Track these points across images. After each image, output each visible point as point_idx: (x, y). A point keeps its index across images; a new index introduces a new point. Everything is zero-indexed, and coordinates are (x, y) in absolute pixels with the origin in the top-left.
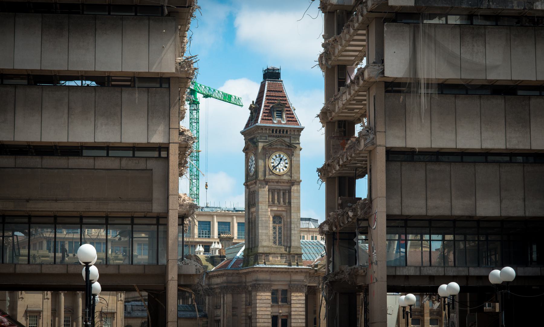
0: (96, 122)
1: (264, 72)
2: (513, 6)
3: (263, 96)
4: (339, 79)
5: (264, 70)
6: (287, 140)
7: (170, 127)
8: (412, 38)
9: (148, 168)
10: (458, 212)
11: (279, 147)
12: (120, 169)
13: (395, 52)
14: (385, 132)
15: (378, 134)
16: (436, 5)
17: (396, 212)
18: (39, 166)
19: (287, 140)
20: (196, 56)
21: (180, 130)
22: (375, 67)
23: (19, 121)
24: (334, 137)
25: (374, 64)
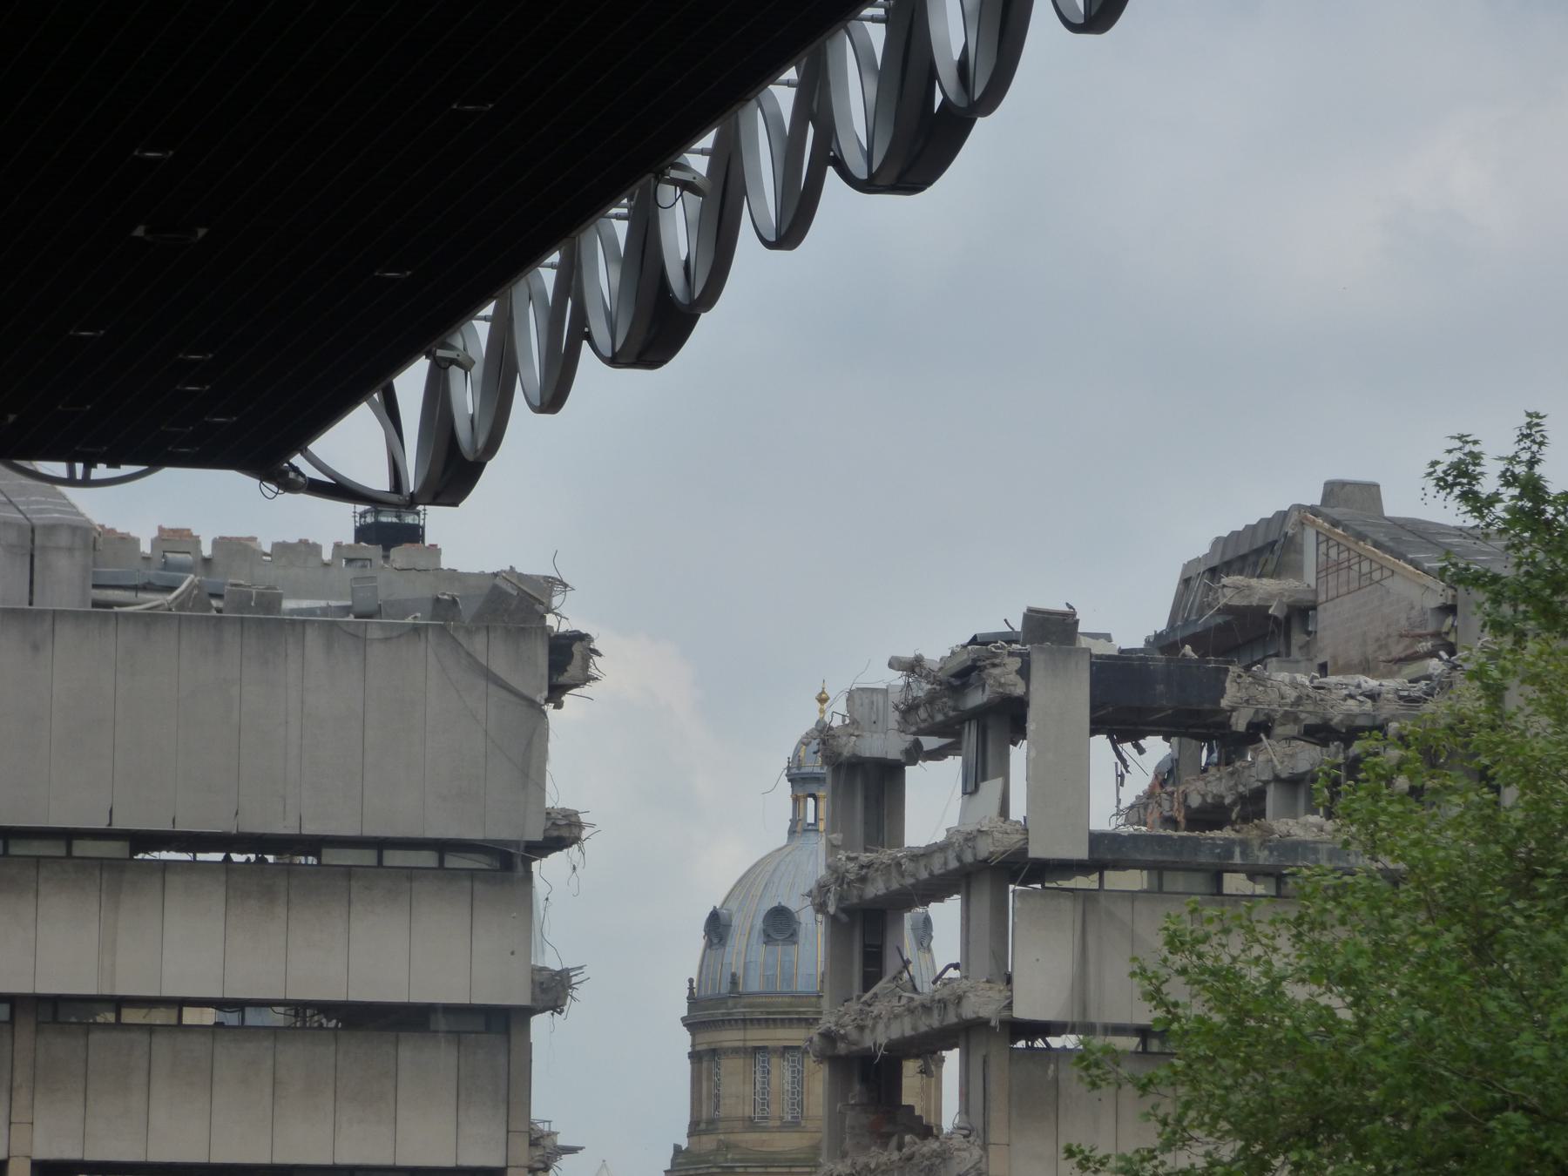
0: (337, 1114)
1: (357, 519)
4: (865, 946)
7: (510, 1129)
8: (1078, 926)
13: (1038, 960)
14: (1008, 1145)
15: (992, 1148)
16: (1138, 857)
20: (581, 968)
21: (530, 1135)
22: (990, 993)
24: (852, 1105)
25: (988, 985)
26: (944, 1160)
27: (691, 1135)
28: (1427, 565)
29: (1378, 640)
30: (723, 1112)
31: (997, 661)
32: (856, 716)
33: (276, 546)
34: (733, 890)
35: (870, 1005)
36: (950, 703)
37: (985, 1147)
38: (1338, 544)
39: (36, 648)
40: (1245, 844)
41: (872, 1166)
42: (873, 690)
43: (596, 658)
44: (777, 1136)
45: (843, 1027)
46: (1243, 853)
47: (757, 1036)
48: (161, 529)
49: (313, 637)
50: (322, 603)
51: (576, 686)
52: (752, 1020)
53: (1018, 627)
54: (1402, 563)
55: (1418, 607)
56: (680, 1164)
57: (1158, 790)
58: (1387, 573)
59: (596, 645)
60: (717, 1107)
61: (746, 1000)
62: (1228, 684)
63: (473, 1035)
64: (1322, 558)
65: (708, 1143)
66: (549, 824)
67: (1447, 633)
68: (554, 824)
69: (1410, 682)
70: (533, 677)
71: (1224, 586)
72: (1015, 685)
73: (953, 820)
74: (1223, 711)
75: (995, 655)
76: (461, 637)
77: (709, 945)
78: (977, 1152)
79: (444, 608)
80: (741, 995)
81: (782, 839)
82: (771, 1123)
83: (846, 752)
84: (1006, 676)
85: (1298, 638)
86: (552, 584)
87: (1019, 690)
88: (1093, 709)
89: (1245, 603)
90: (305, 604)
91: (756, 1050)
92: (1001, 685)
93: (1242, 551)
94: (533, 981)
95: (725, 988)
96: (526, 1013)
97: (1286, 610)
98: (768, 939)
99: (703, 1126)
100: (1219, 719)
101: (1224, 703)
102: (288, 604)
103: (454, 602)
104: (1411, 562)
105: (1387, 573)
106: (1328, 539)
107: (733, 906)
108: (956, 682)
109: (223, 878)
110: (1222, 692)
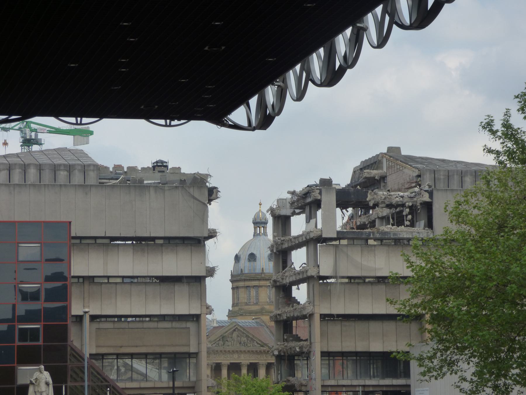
2: (390, 236)
4: (283, 259)
5: (153, 162)
9: (187, 327)
10: (359, 349)
12: (172, 328)
16: (348, 236)
17: (325, 350)
18: (127, 327)
22: (314, 270)
26: (304, 309)
27: (232, 307)
28: (413, 166)
29: (402, 184)
30: (240, 301)
31: (314, 191)
32: (279, 205)
33: (142, 168)
34: (240, 250)
35: (284, 273)
36: (303, 201)
37: (314, 306)
38: (392, 162)
39: (86, 194)
40: (373, 233)
41: (286, 311)
42: (283, 199)
43: (219, 193)
44: (253, 306)
45: (278, 279)
46: (373, 235)
47: (248, 283)
48: (115, 165)
49: (152, 191)
50: (153, 182)
51: (215, 199)
52: (246, 280)
53: (318, 183)
54: (407, 165)
55: (411, 176)
56: (230, 314)
57: (349, 221)
58: (403, 168)
59: (219, 190)
60: (238, 300)
61: (245, 275)
62: (368, 195)
63: (192, 283)
64: (388, 165)
65: (237, 308)
66: (209, 232)
67: (419, 182)
68: (210, 232)
69: (411, 193)
70: (204, 198)
71: (365, 172)
72: (318, 196)
73: (304, 229)
74: (367, 201)
75: (313, 190)
76: (187, 189)
77: (236, 262)
78: (312, 307)
79: (183, 182)
80: (243, 274)
81: (252, 237)
82: (251, 304)
83: (277, 214)
84: (316, 195)
85: (382, 184)
86: (208, 175)
87: (319, 198)
88: (337, 201)
89: (369, 176)
90: (149, 182)
91: (247, 287)
92: (315, 197)
93: (368, 164)
94: (206, 270)
95: (240, 272)
96: (205, 277)
97: (379, 178)
98: (249, 260)
99: (235, 305)
100: (366, 203)
101: (368, 199)
102: (145, 182)
103: (185, 180)
104: (409, 165)
105: (403, 168)
106: (389, 160)
107: (241, 253)
108: (304, 196)
109: (132, 247)
110: (367, 197)
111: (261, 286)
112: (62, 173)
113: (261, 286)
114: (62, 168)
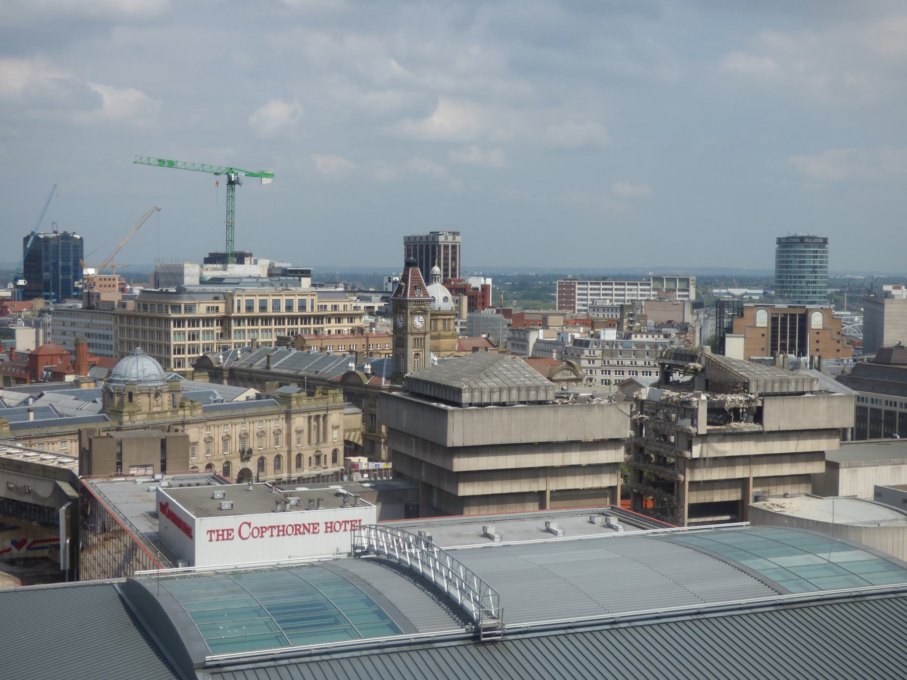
3: (408, 279)
6: (423, 307)
10: (707, 501)
11: (419, 311)
19: (423, 307)
23: (568, 481)
49: (596, 407)
111: (439, 319)
112: (532, 392)
113: (439, 319)
114: (533, 389)
